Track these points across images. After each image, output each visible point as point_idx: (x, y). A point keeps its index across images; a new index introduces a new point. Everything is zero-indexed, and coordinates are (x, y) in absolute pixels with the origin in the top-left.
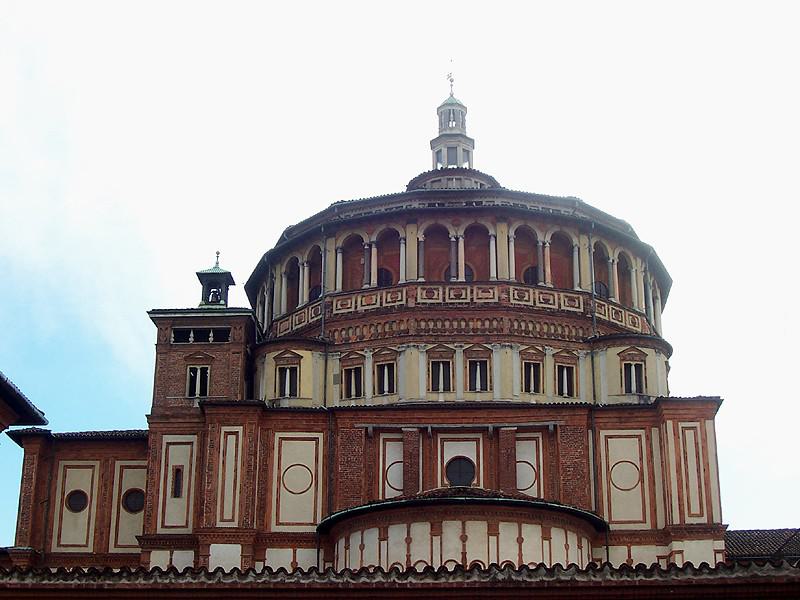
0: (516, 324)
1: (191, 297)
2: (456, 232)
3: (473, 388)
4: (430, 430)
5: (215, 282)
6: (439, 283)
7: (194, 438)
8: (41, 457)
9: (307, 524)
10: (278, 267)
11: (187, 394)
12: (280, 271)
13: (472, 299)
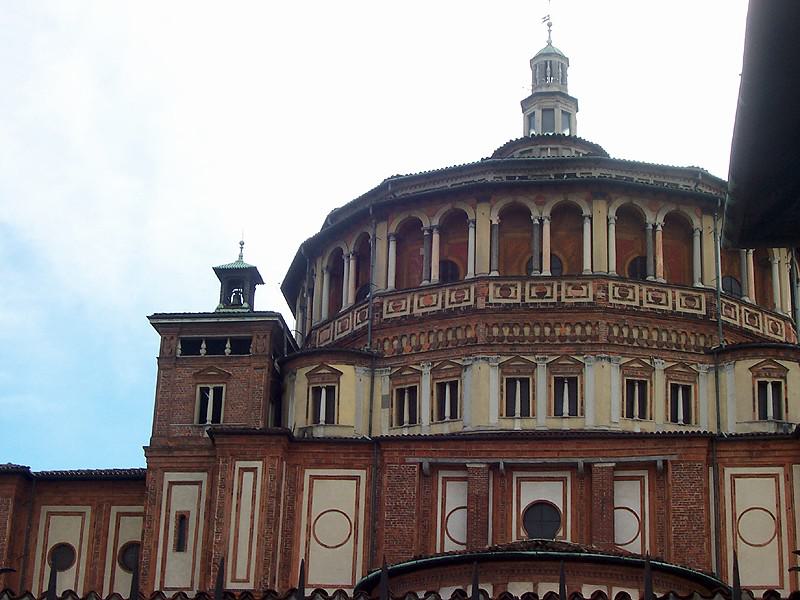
0: (616, 331)
1: (205, 298)
2: (541, 213)
3: (558, 413)
4: (502, 466)
5: (238, 280)
6: (519, 278)
7: (203, 477)
8: (17, 501)
10: (319, 262)
11: (196, 420)
12: (323, 263)
13: (559, 298)
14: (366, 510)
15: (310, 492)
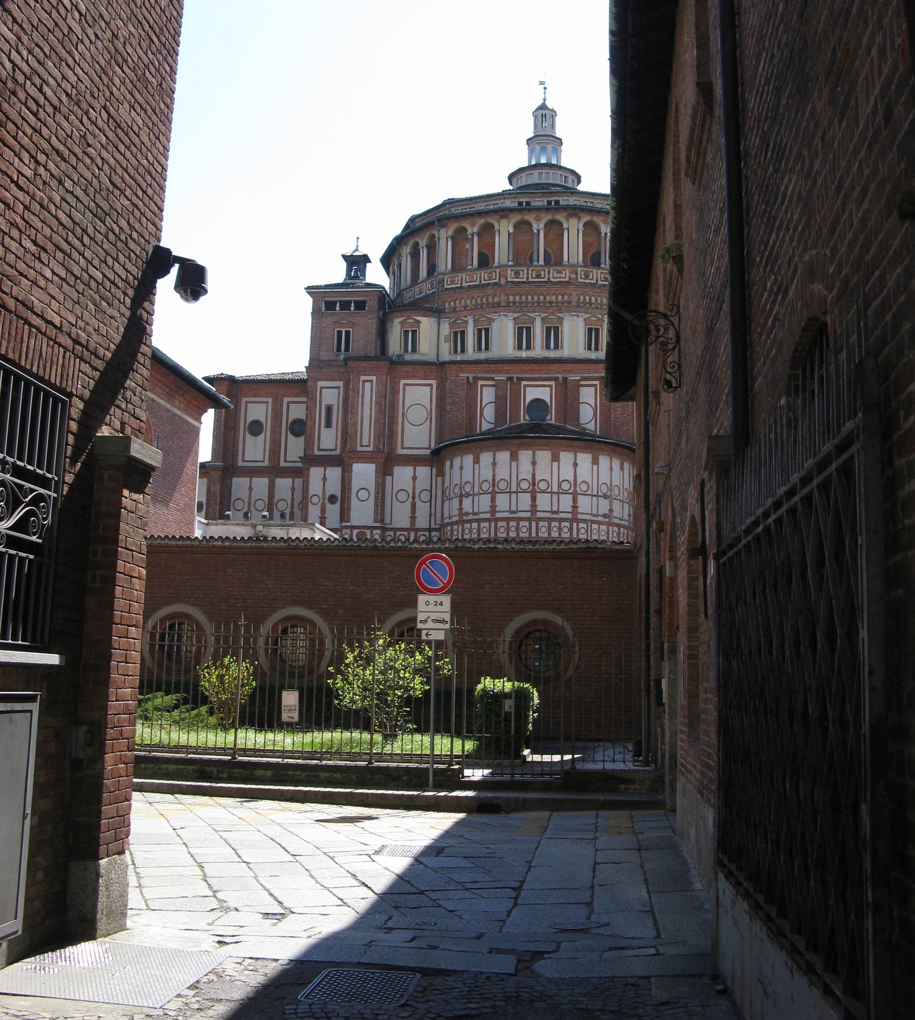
0: (582, 298)
1: (337, 274)
2: (538, 226)
3: (548, 347)
4: (515, 379)
5: (357, 263)
7: (340, 384)
9: (424, 448)
10: (404, 248)
11: (335, 350)
12: (406, 251)
13: (549, 279)
14: (437, 404)
15: (404, 394)
